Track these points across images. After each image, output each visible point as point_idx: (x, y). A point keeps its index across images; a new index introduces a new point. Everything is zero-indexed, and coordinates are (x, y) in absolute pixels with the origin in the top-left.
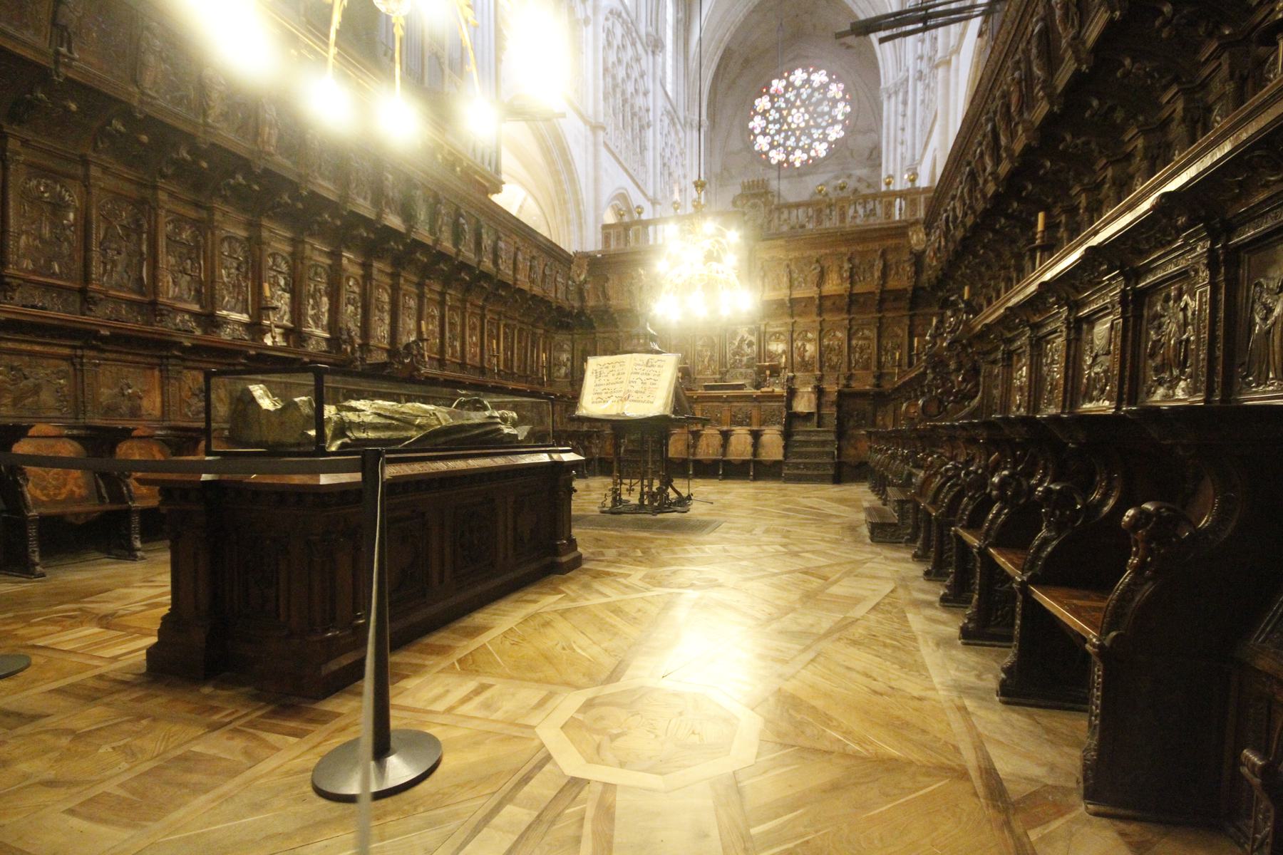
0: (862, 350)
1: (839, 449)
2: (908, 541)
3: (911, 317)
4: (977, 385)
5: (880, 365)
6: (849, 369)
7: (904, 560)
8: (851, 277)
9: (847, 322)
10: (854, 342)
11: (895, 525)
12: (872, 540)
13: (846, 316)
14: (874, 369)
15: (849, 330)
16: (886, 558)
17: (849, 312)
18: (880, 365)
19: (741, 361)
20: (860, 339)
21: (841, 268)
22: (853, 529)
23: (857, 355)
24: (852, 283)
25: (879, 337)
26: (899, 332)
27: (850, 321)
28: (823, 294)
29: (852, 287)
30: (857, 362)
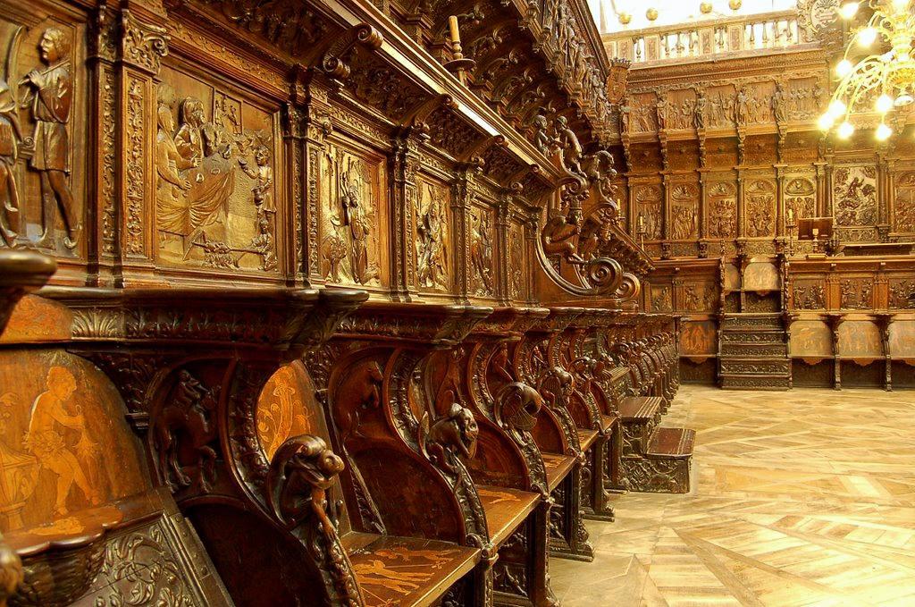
19: (853, 215)
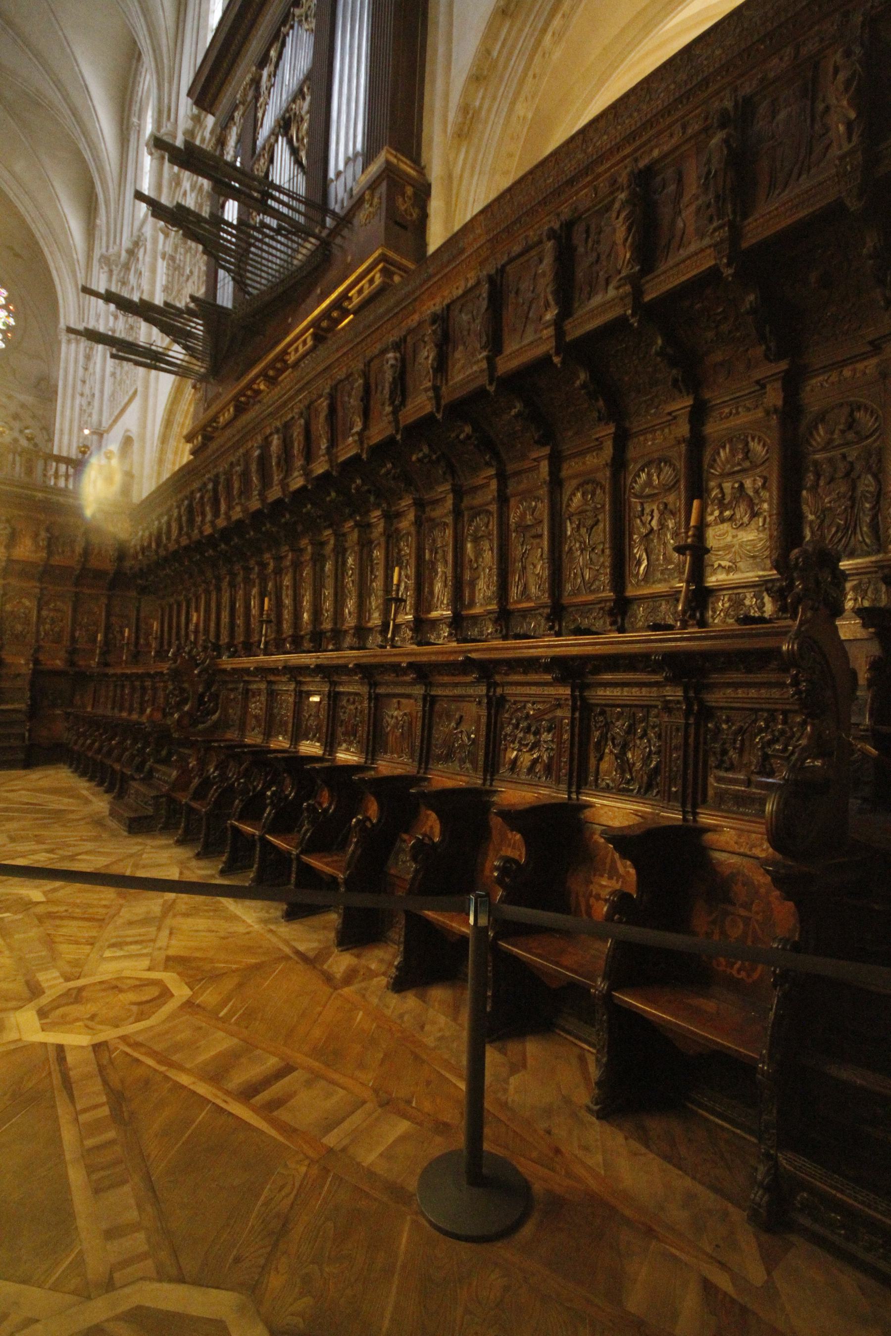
0: (53, 621)
1: (30, 731)
2: (162, 828)
3: (109, 598)
4: (217, 704)
5: (73, 639)
6: (37, 641)
7: (168, 846)
8: (49, 546)
9: (37, 590)
10: (44, 613)
11: (151, 817)
12: (130, 832)
13: (38, 585)
14: (66, 641)
15: (40, 599)
16: (152, 847)
17: (40, 580)
18: (73, 639)
20: (50, 610)
21: (37, 535)
22: (99, 823)
23: (47, 627)
24: (50, 554)
25: (75, 610)
26: (96, 609)
27: (41, 589)
28: (14, 558)
29: (48, 559)
30: (46, 634)
